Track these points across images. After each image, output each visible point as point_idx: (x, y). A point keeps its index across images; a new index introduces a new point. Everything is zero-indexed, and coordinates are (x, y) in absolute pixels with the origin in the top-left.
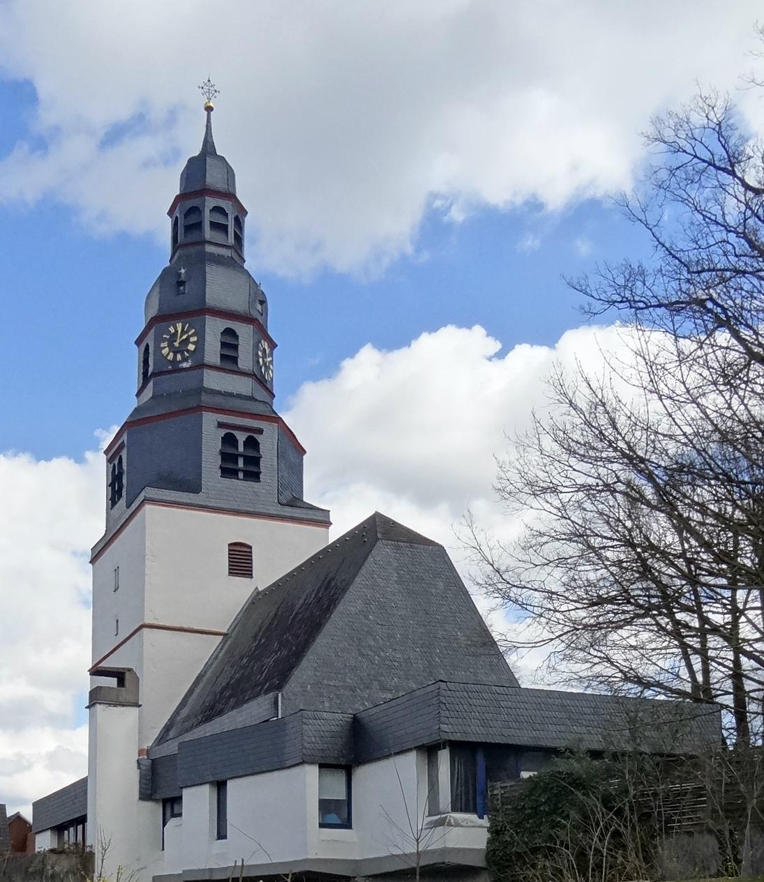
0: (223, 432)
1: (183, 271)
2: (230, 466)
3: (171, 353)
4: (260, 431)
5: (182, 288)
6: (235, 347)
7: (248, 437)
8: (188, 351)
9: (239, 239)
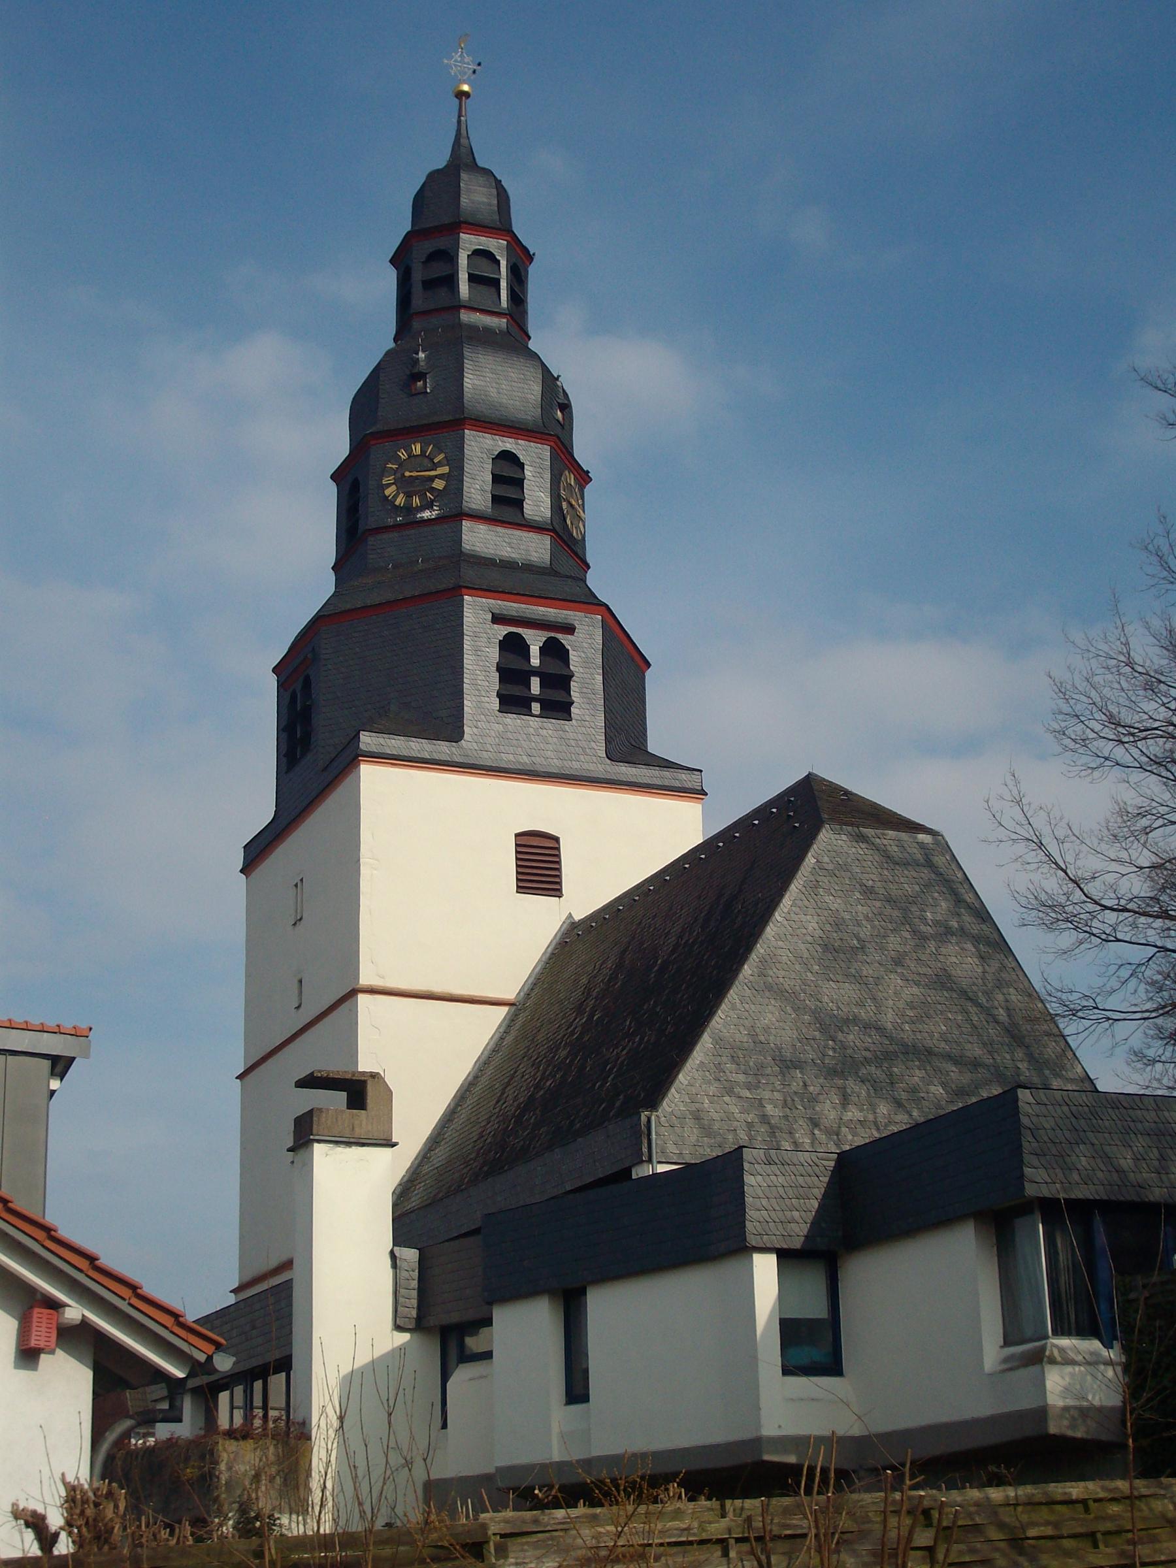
0: (503, 631)
1: (422, 355)
2: (516, 690)
3: (401, 495)
4: (570, 629)
5: (420, 384)
6: (519, 483)
7: (549, 639)
8: (432, 490)
9: (518, 299)
